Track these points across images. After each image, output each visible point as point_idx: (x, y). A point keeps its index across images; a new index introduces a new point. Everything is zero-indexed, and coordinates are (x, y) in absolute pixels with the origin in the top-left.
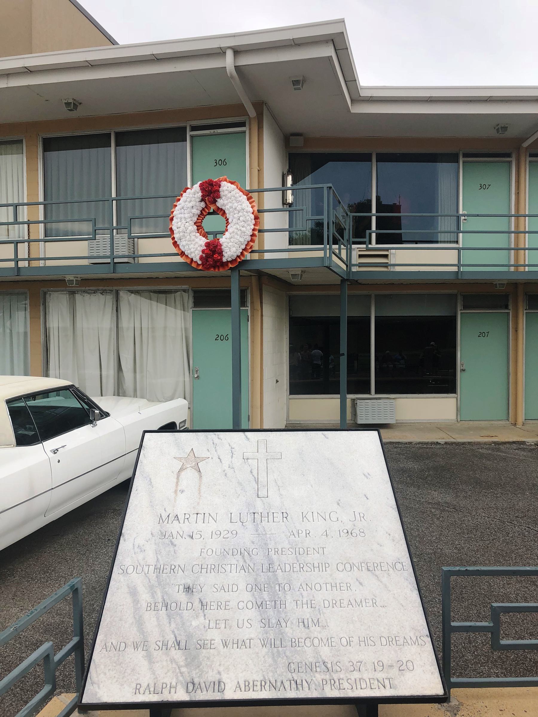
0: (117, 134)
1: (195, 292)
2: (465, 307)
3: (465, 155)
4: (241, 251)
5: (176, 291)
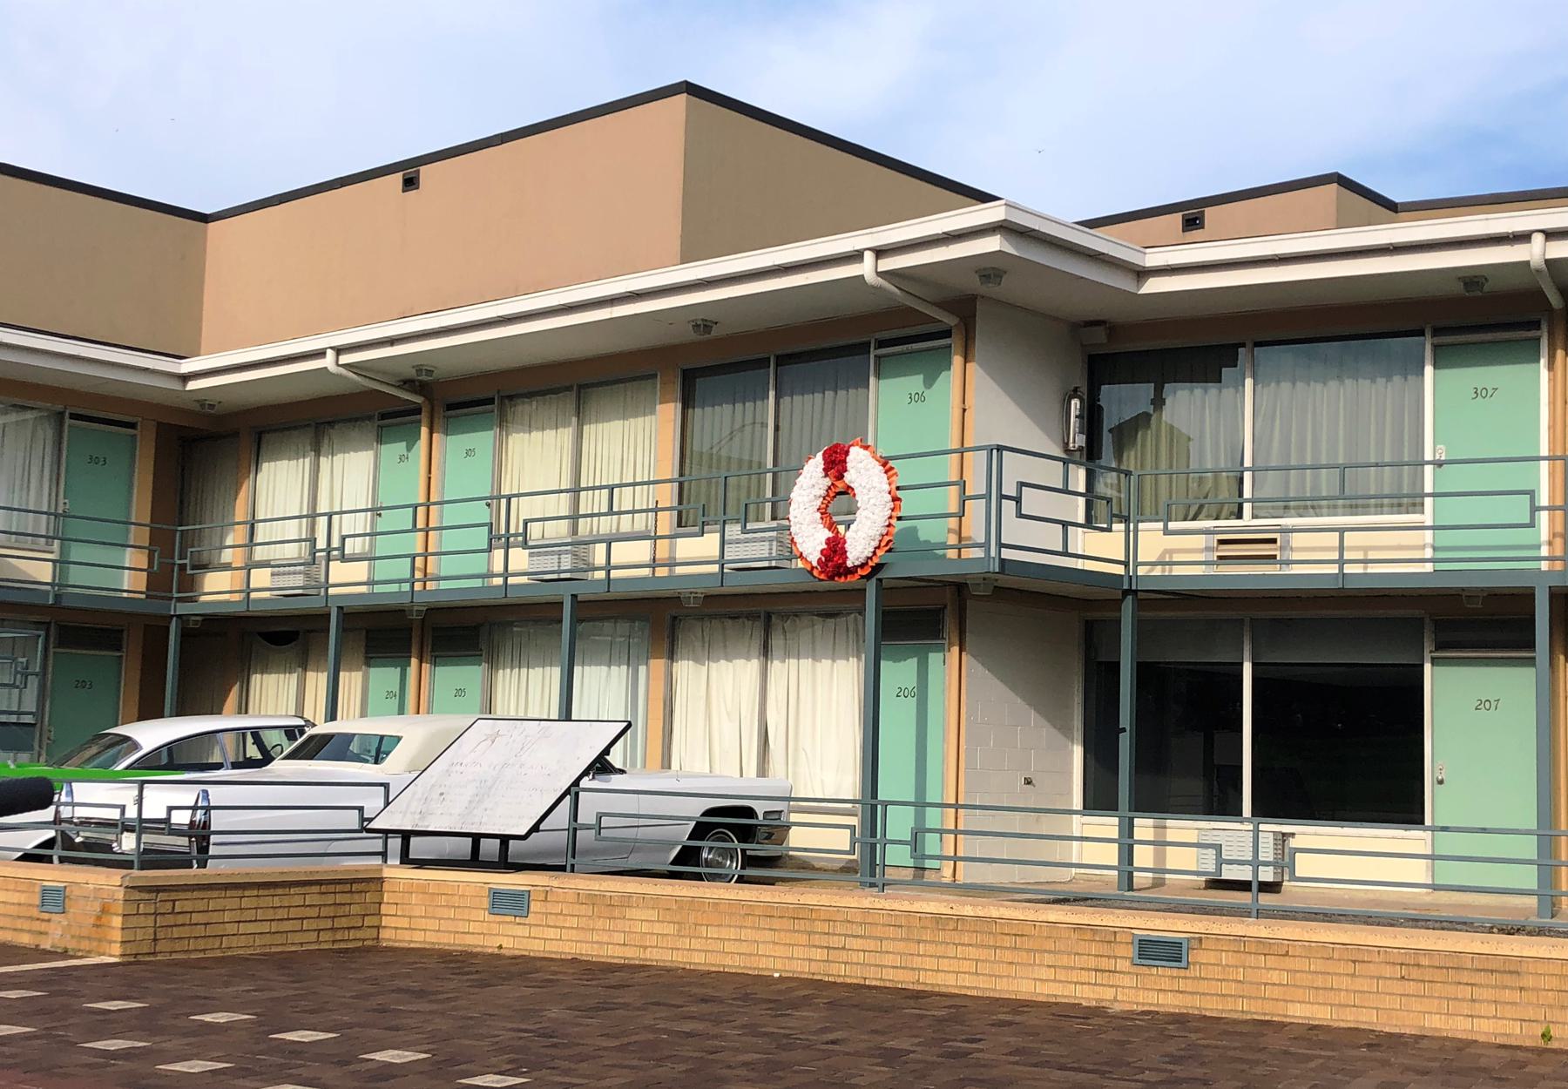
2: (1439, 647)
4: (873, 550)
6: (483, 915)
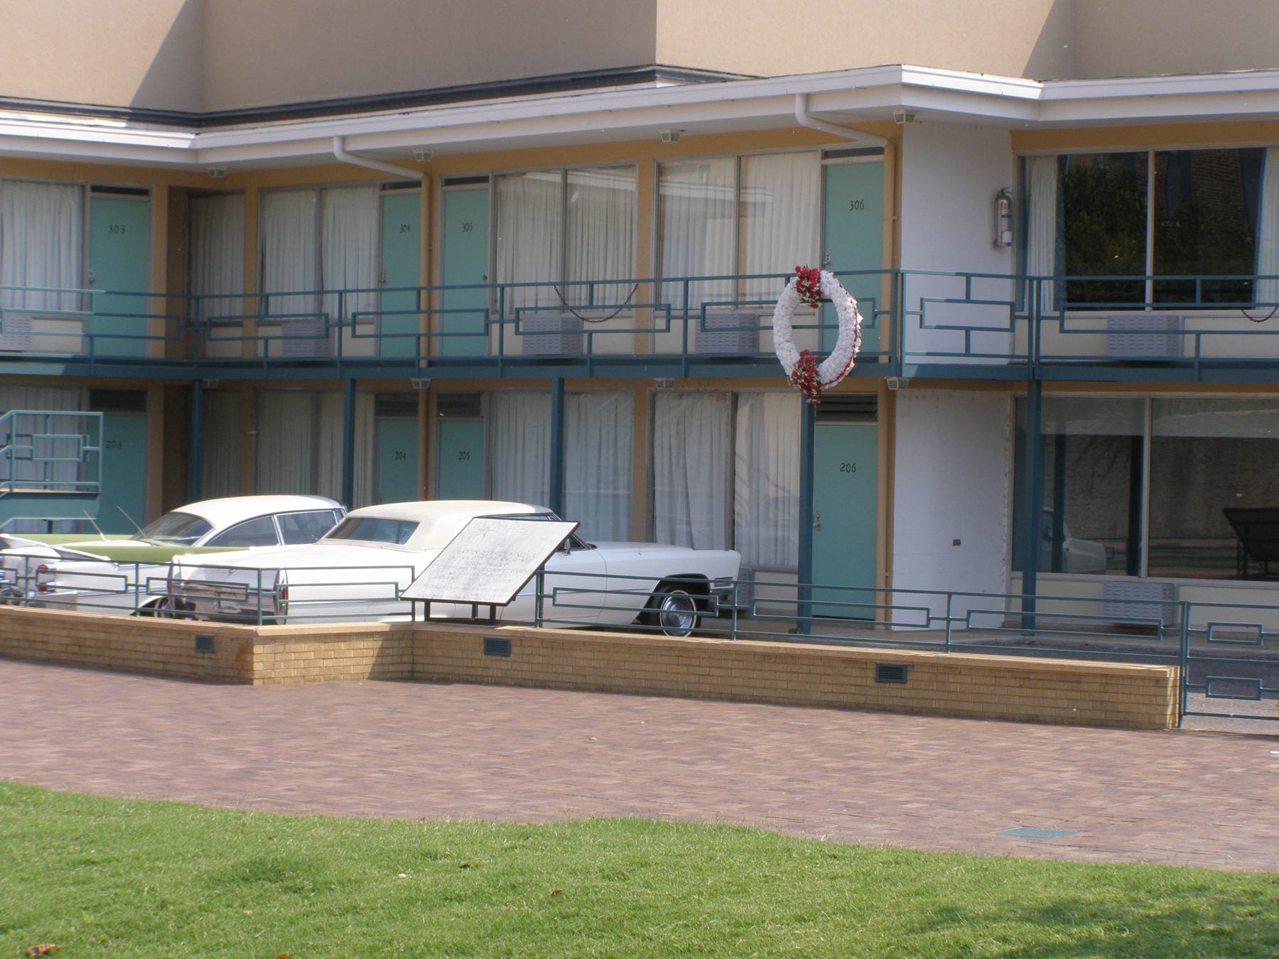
6: (481, 655)
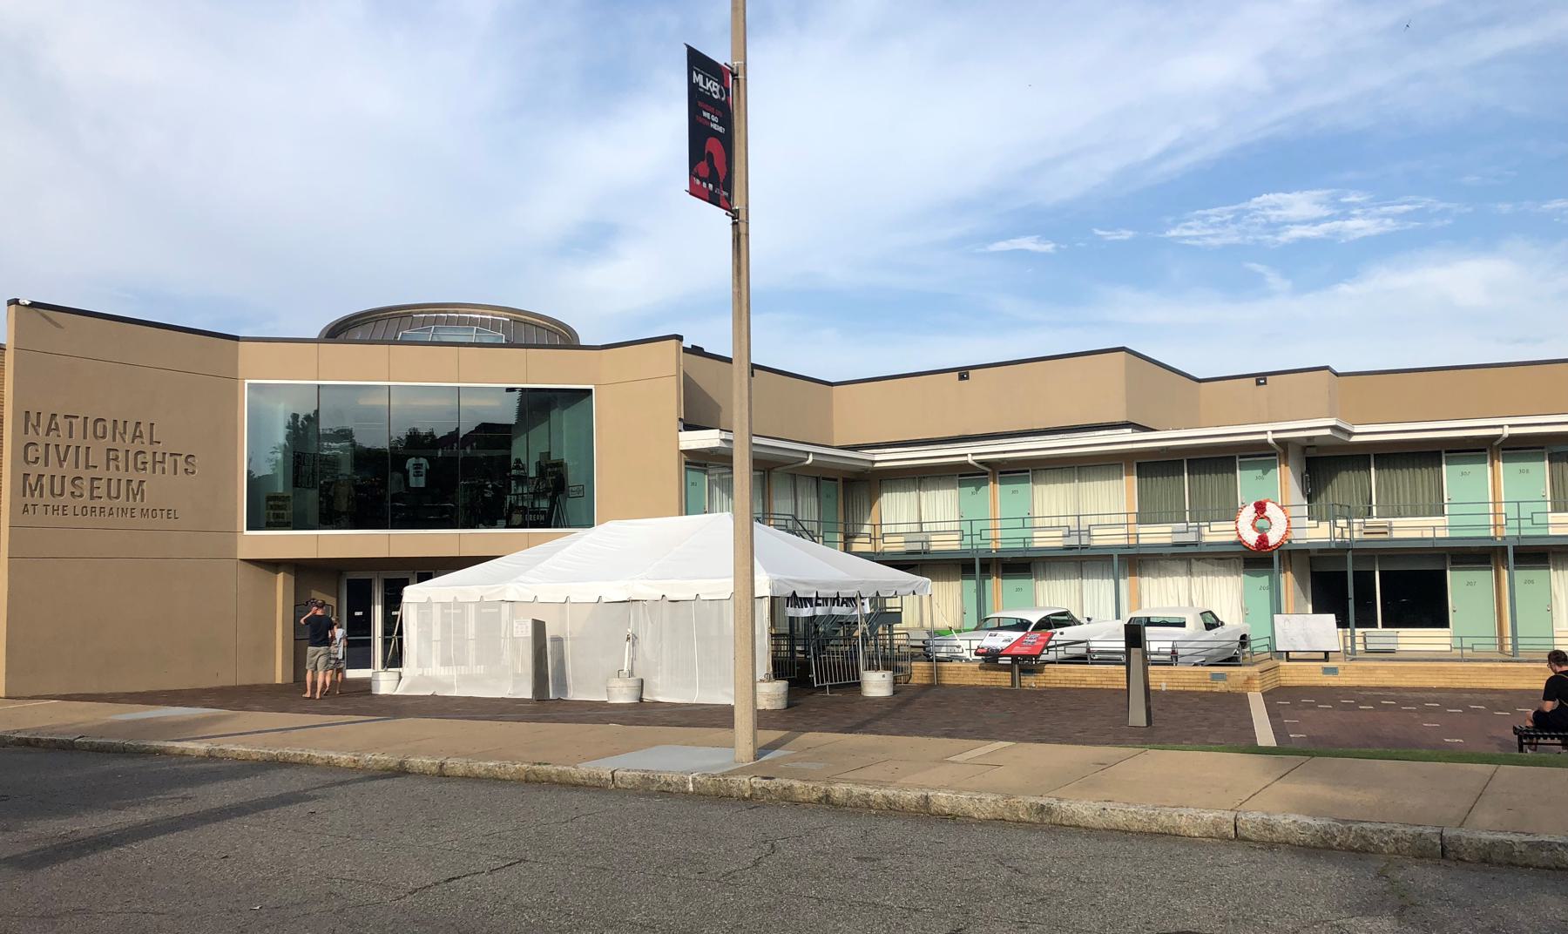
0: (1188, 460)
1: (1245, 559)
2: (1453, 563)
3: (1446, 452)
5: (1231, 558)
